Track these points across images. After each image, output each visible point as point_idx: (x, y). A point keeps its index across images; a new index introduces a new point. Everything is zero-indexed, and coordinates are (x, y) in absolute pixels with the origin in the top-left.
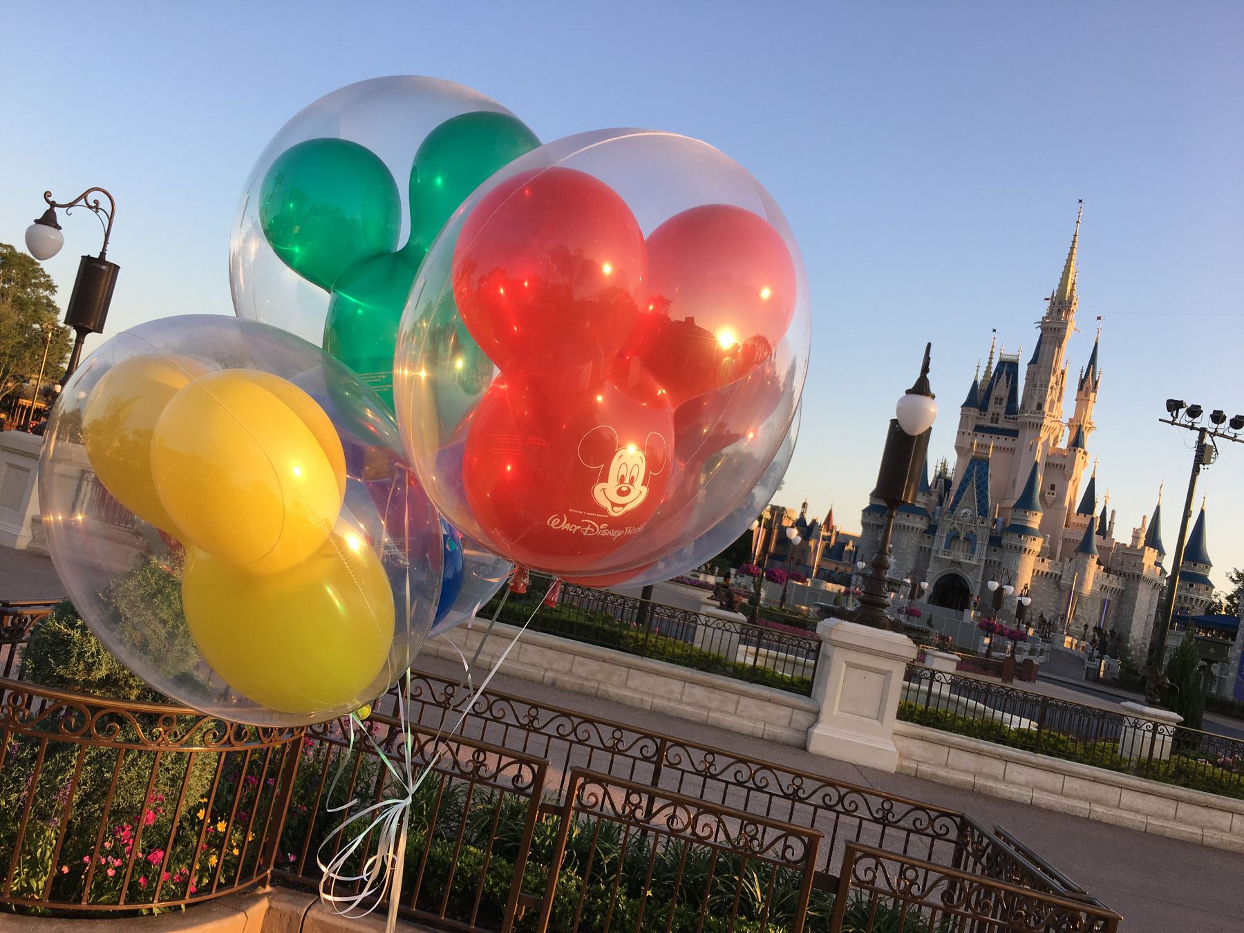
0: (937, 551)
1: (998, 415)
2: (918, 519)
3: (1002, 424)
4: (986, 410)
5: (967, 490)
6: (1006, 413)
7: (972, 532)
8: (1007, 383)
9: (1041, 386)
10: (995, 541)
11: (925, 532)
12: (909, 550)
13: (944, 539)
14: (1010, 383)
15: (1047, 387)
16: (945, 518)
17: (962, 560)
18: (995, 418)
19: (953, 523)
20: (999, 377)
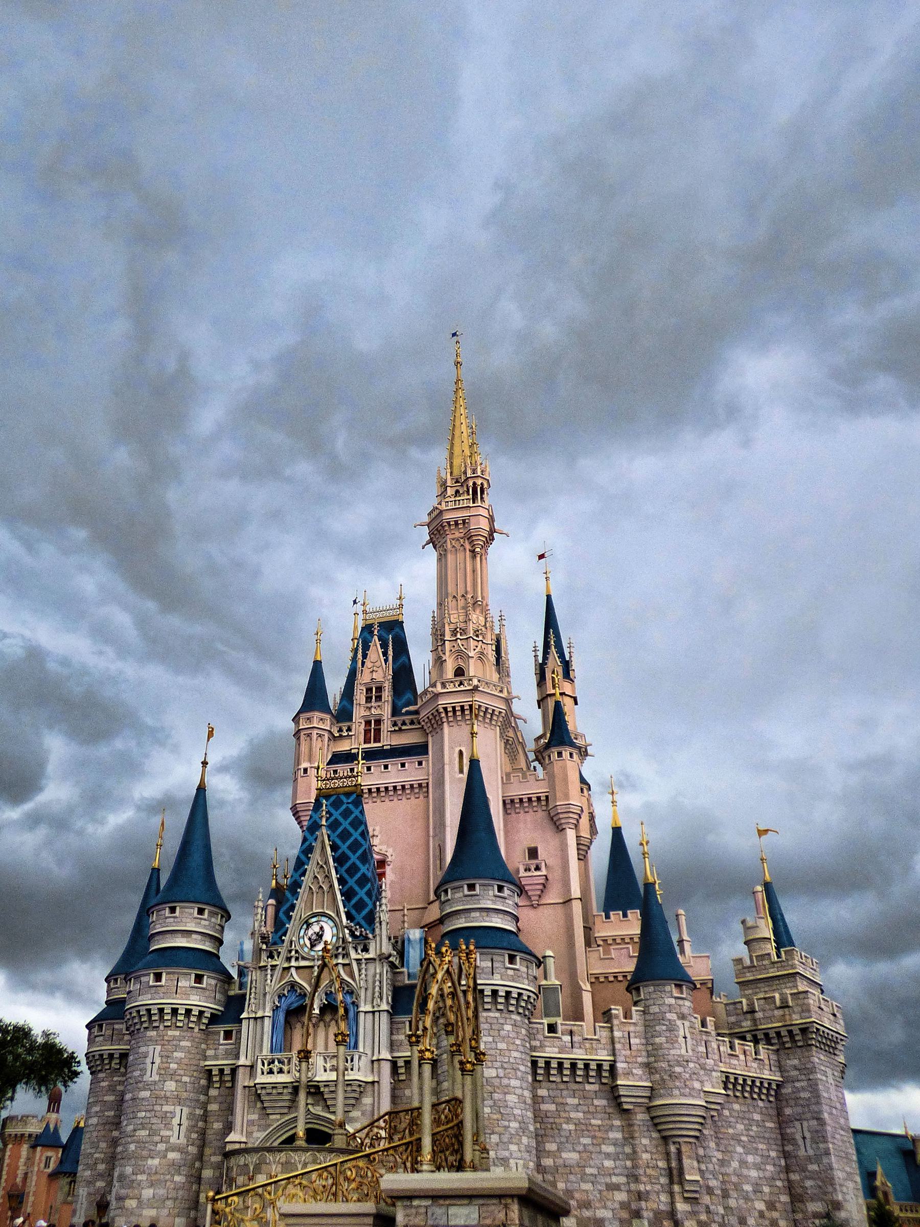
1: (378, 722)
2: (187, 982)
3: (388, 740)
5: (311, 868)
6: (393, 715)
8: (385, 654)
9: (454, 632)
11: (215, 1019)
12: (170, 1086)
13: (267, 1023)
14: (390, 652)
15: (464, 631)
16: (262, 964)
18: (373, 729)
20: (366, 648)
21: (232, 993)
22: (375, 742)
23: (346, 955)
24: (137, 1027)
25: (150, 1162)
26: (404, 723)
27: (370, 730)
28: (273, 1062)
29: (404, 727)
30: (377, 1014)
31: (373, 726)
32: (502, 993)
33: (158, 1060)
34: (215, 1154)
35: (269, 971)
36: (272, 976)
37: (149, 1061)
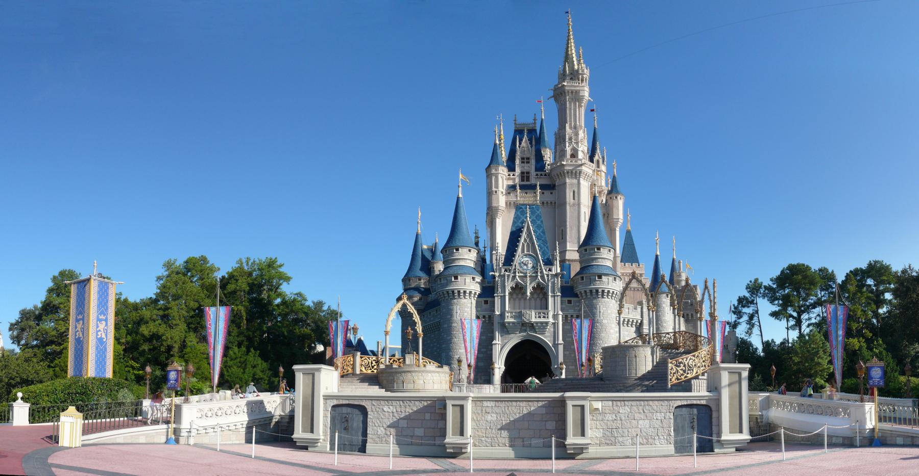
0: (502, 315)
1: (528, 173)
4: (514, 170)
5: (524, 235)
6: (536, 171)
7: (539, 284)
8: (531, 143)
10: (568, 292)
14: (534, 143)
17: (533, 320)
18: (524, 176)
19: (514, 277)
20: (521, 140)
21: (484, 285)
22: (527, 181)
23: (542, 272)
24: (443, 299)
25: (460, 351)
26: (541, 175)
27: (524, 176)
28: (540, 313)
29: (541, 176)
30: (556, 298)
31: (525, 175)
32: (611, 292)
33: (459, 312)
34: (483, 348)
35: (506, 277)
36: (507, 279)
37: (455, 311)
